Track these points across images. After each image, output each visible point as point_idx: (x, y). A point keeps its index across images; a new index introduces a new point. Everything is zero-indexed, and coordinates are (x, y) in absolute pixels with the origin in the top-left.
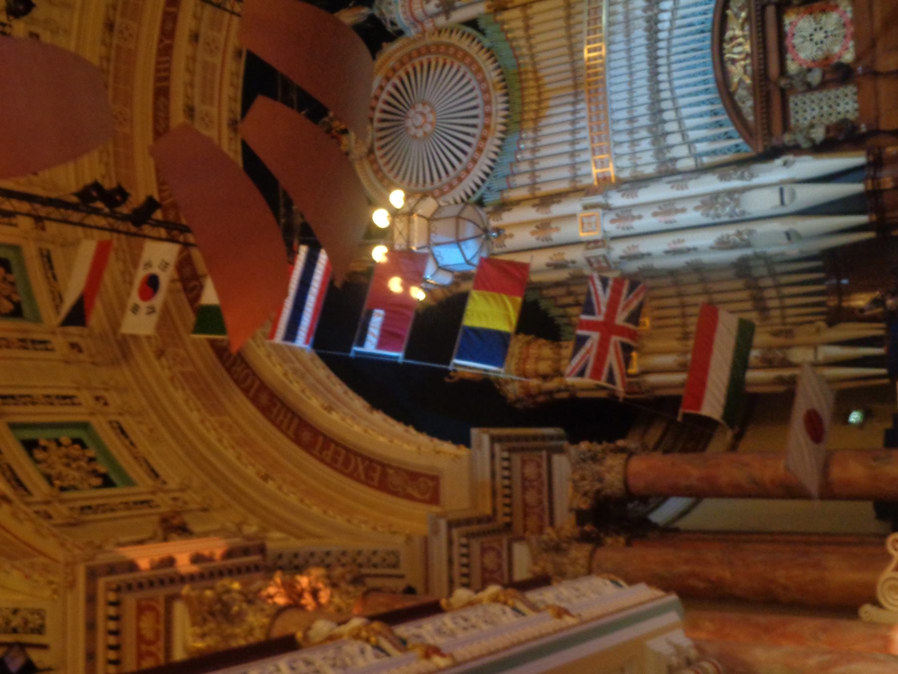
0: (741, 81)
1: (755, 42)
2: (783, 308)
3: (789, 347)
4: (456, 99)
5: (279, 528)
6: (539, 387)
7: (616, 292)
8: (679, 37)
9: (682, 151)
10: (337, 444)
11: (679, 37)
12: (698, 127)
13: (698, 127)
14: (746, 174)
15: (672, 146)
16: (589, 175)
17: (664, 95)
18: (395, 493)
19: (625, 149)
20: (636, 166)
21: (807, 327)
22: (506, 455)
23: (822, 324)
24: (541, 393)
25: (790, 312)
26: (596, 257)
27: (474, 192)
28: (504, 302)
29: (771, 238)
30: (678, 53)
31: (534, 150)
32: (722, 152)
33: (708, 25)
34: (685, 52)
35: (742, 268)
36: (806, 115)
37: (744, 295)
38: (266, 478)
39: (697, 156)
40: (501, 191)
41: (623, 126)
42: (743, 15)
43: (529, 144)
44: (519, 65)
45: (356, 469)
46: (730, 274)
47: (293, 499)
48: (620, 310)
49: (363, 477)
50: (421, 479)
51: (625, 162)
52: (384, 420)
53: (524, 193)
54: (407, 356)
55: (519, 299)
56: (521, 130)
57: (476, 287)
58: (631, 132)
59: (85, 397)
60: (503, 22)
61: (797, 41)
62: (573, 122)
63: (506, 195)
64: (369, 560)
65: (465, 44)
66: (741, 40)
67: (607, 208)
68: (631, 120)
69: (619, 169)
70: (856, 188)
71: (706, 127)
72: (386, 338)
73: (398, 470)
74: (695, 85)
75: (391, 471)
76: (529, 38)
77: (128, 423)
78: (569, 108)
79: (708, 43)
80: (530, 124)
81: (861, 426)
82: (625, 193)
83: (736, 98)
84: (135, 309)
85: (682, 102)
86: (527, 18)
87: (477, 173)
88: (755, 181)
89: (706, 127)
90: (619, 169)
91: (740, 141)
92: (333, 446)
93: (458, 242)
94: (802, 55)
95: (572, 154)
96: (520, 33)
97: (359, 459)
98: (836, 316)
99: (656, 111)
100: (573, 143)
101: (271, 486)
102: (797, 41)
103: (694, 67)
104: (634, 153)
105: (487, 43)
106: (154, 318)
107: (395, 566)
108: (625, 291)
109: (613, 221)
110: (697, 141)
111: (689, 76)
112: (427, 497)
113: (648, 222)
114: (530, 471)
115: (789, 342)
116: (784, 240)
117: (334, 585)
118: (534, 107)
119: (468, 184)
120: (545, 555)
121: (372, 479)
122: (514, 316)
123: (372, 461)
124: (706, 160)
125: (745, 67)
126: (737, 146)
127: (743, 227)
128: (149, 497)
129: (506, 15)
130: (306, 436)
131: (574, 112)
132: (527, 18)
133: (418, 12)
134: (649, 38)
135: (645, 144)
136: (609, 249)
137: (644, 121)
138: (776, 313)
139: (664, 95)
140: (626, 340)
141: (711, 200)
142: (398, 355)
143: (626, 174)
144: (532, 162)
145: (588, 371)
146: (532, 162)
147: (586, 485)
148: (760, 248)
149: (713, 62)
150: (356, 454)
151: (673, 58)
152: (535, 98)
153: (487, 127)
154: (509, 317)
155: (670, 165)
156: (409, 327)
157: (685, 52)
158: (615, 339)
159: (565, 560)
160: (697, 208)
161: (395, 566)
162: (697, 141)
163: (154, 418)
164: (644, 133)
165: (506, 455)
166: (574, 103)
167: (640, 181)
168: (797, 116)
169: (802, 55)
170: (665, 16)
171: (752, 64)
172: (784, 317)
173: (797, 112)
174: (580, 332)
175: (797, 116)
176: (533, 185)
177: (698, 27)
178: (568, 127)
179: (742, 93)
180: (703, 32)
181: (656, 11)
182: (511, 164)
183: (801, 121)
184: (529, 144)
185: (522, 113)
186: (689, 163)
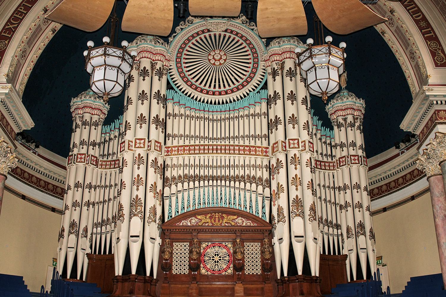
2: (101, 233)
3: (77, 236)
4: (212, 77)
8: (230, 191)
10: (26, 14)
21: (88, 244)
23: (89, 251)
25: (99, 237)
27: (176, 85)
33: (232, 206)
39: (169, 197)
49: (7, 27)
53: (170, 110)
65: (254, 82)
66: (221, 221)
76: (248, 116)
86: (259, 115)
87: (184, 87)
96: (252, 111)
97: (16, 25)
103: (213, 199)
105: (251, 94)
115: (80, 235)
119: (180, 82)
127: (126, 217)
129: (264, 105)
132: (259, 115)
133: (272, 59)
134: (206, 176)
150: (19, 24)
152: (215, 118)
171: (208, 226)
180: (229, 204)
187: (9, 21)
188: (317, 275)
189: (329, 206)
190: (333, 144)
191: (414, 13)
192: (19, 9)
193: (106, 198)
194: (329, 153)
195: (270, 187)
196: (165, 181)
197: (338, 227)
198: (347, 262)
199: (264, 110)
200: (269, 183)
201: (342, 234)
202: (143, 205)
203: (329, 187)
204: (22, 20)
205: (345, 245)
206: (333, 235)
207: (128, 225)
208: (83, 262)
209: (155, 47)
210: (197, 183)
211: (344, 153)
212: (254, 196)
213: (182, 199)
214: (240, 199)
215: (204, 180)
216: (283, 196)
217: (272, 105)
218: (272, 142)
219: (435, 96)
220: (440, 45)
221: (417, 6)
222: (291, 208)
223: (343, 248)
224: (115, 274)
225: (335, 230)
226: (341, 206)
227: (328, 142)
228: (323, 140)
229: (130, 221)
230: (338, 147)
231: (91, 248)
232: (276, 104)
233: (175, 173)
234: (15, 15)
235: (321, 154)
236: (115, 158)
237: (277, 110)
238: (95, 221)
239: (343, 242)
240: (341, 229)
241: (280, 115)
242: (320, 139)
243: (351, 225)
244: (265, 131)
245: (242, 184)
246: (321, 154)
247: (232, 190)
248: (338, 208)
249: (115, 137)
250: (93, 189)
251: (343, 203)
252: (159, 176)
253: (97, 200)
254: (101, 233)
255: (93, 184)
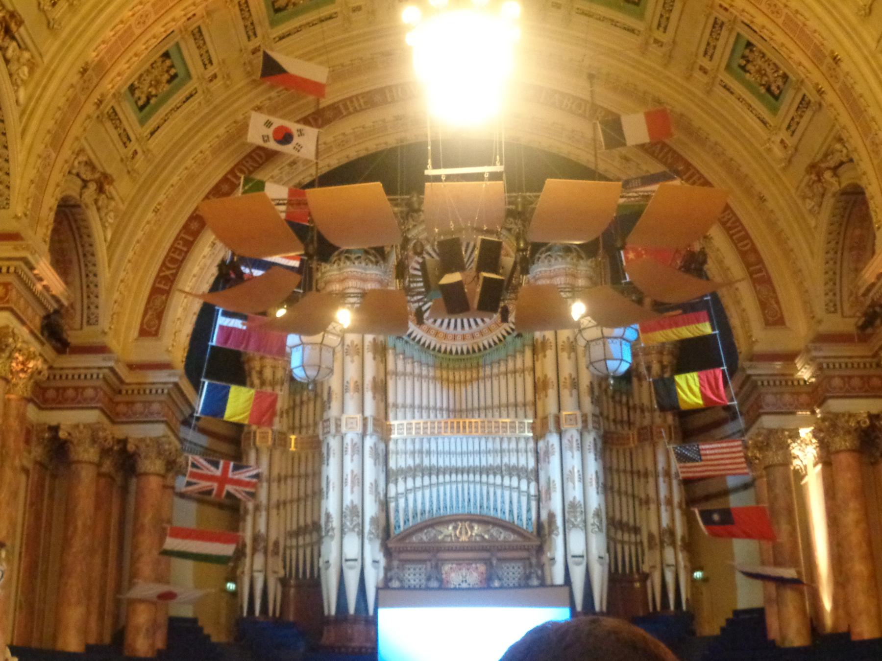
0: (441, 533)
1: (466, 545)
2: (298, 547)
5: (114, 235)
6: (254, 368)
7: (248, 484)
8: (481, 490)
9: (401, 488)
10: (187, 252)
11: (481, 490)
12: (415, 501)
13: (415, 501)
14: (372, 536)
15: (405, 482)
16: (396, 418)
17: (441, 478)
18: (148, 302)
19: (410, 447)
20: (397, 453)
21: (281, 564)
22: (166, 391)
23: (282, 573)
24: (251, 369)
25: (294, 551)
26: (329, 426)
28: (244, 413)
29: (330, 551)
30: (469, 489)
31: (420, 376)
32: (397, 516)
33: (485, 511)
34: (469, 494)
35: (316, 527)
36: (412, 576)
37: (302, 523)
38: (156, 211)
39: (396, 499)
40: (395, 347)
41: (426, 446)
42: (486, 537)
43: (424, 373)
44: (484, 366)
45: (168, 269)
46: (316, 519)
47: (140, 234)
48: (235, 487)
49: (162, 274)
50: (157, 322)
51: (401, 446)
52: (213, 275)
54: (213, 347)
55: (246, 422)
56: (434, 367)
57: (257, 393)
58: (421, 452)
59: (211, 70)
60: (523, 352)
61: (464, 572)
62: (435, 408)
63: (390, 351)
64: (92, 303)
66: (469, 533)
67: (363, 435)
68: (429, 453)
69: (396, 441)
70: (352, 610)
71: (415, 506)
72: (227, 332)
73: (164, 303)
74: (445, 500)
75: (164, 297)
77: (198, 98)
78: (445, 405)
79: (473, 511)
80: (438, 374)
81: (225, 591)
82: (375, 449)
83: (430, 529)
84: (268, 124)
85: (434, 490)
88: (366, 541)
89: (415, 506)
90: (396, 441)
91: (402, 529)
92: (185, 249)
93: (303, 366)
94: (453, 575)
95: (413, 406)
97: (174, 271)
98: (284, 582)
99: (432, 471)
100: (421, 407)
101: (150, 215)
102: (464, 572)
104: (406, 453)
105: (509, 338)
106: (260, 142)
107: (89, 323)
108: (248, 489)
109: (352, 440)
110: (406, 500)
111: (451, 497)
112: (145, 327)
113: (350, 466)
114: (156, 407)
116: (326, 559)
117: (30, 378)
118: (451, 377)
120: (90, 432)
121: (159, 283)
122: (235, 419)
123: (172, 282)
124: (392, 505)
125: (450, 536)
126: (399, 527)
127: (337, 532)
128: (132, 137)
129: (528, 353)
130: (194, 226)
131: (441, 409)
135: (410, 462)
136: (334, 436)
137: (426, 462)
138: (294, 542)
139: (447, 477)
140: (214, 492)
141: (357, 511)
142: (214, 342)
143: (392, 446)
144: (412, 374)
145: (195, 470)
146: (412, 374)
147: (143, 447)
148: (326, 541)
149: (459, 515)
150: (178, 268)
151: (466, 486)
153: (446, 336)
154: (234, 416)
155: (393, 478)
156: (232, 347)
157: (469, 494)
158: (215, 485)
159: (87, 446)
160: (352, 502)
161: (89, 323)
162: (406, 500)
163: (206, 110)
164: (418, 461)
165: (166, 391)
166: (448, 410)
167: (384, 458)
168: (412, 570)
169: (453, 575)
170: (498, 480)
171: (452, 541)
172: (291, 548)
173: (415, 569)
174: (222, 463)
175: (412, 570)
176: (396, 374)
177: (485, 505)
178: (432, 404)
179: (432, 532)
180: (481, 507)
181: (504, 473)
182: (413, 358)
183: (408, 572)
184: (424, 373)
185: (448, 367)
186: (392, 492)
187: (164, 264)
188: (604, 609)
189: (624, 499)
190: (631, 403)
191: (741, 239)
192: (176, 245)
193: (302, 494)
194: (625, 418)
195: (537, 480)
196: (389, 476)
197: (636, 530)
198: (649, 583)
199: (529, 362)
200: (536, 475)
201: (641, 543)
202: (360, 514)
203: (625, 471)
204: (182, 261)
205: (646, 559)
206: (630, 543)
207: (339, 544)
208: (274, 590)
209: (365, 269)
210: (434, 478)
211: (646, 422)
212: (515, 495)
213: (414, 499)
214: (495, 501)
215: (444, 474)
216: (556, 497)
217: (540, 356)
218: (540, 414)
219: (760, 375)
220: (774, 291)
221: (744, 229)
222: (567, 515)
223: (643, 563)
224: (323, 612)
225: (633, 536)
226: (641, 500)
227: (624, 399)
228: (617, 398)
229: (342, 538)
230: (638, 411)
231: (285, 567)
232: (545, 356)
233: (402, 464)
234: (171, 254)
235: (614, 421)
236: (311, 432)
237: (547, 366)
238: (288, 529)
239: (643, 554)
240: (640, 534)
241: (551, 375)
242: (613, 397)
243: (654, 529)
244: (530, 397)
245: (498, 478)
246: (614, 421)
247: (485, 488)
248: (637, 503)
249: (309, 399)
250: (282, 482)
251: (643, 496)
252: (381, 468)
253: (289, 498)
254: (298, 547)
255: (283, 474)
